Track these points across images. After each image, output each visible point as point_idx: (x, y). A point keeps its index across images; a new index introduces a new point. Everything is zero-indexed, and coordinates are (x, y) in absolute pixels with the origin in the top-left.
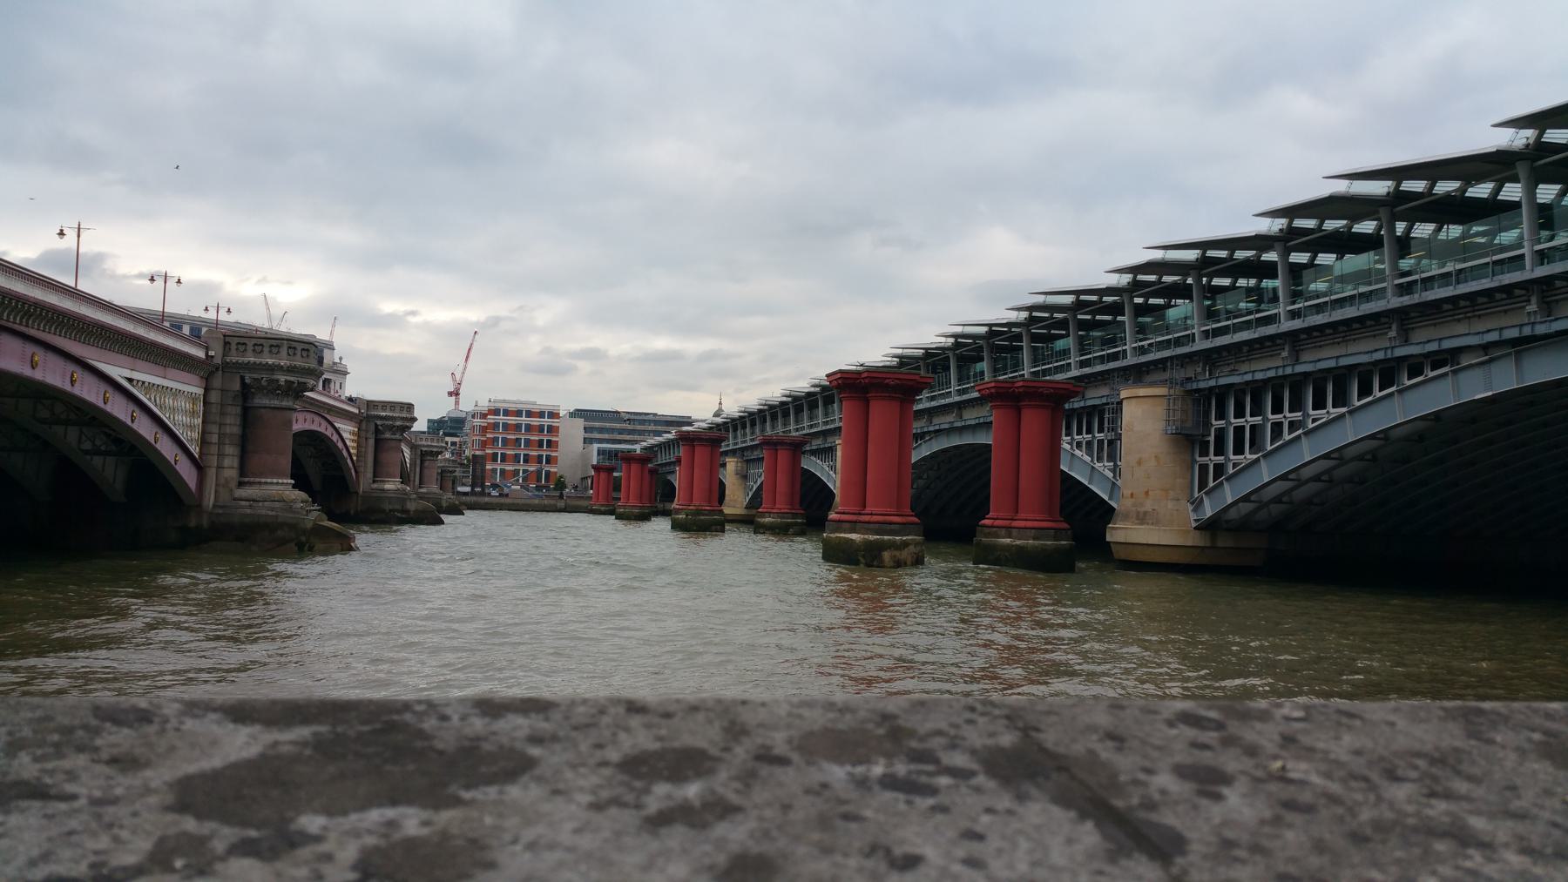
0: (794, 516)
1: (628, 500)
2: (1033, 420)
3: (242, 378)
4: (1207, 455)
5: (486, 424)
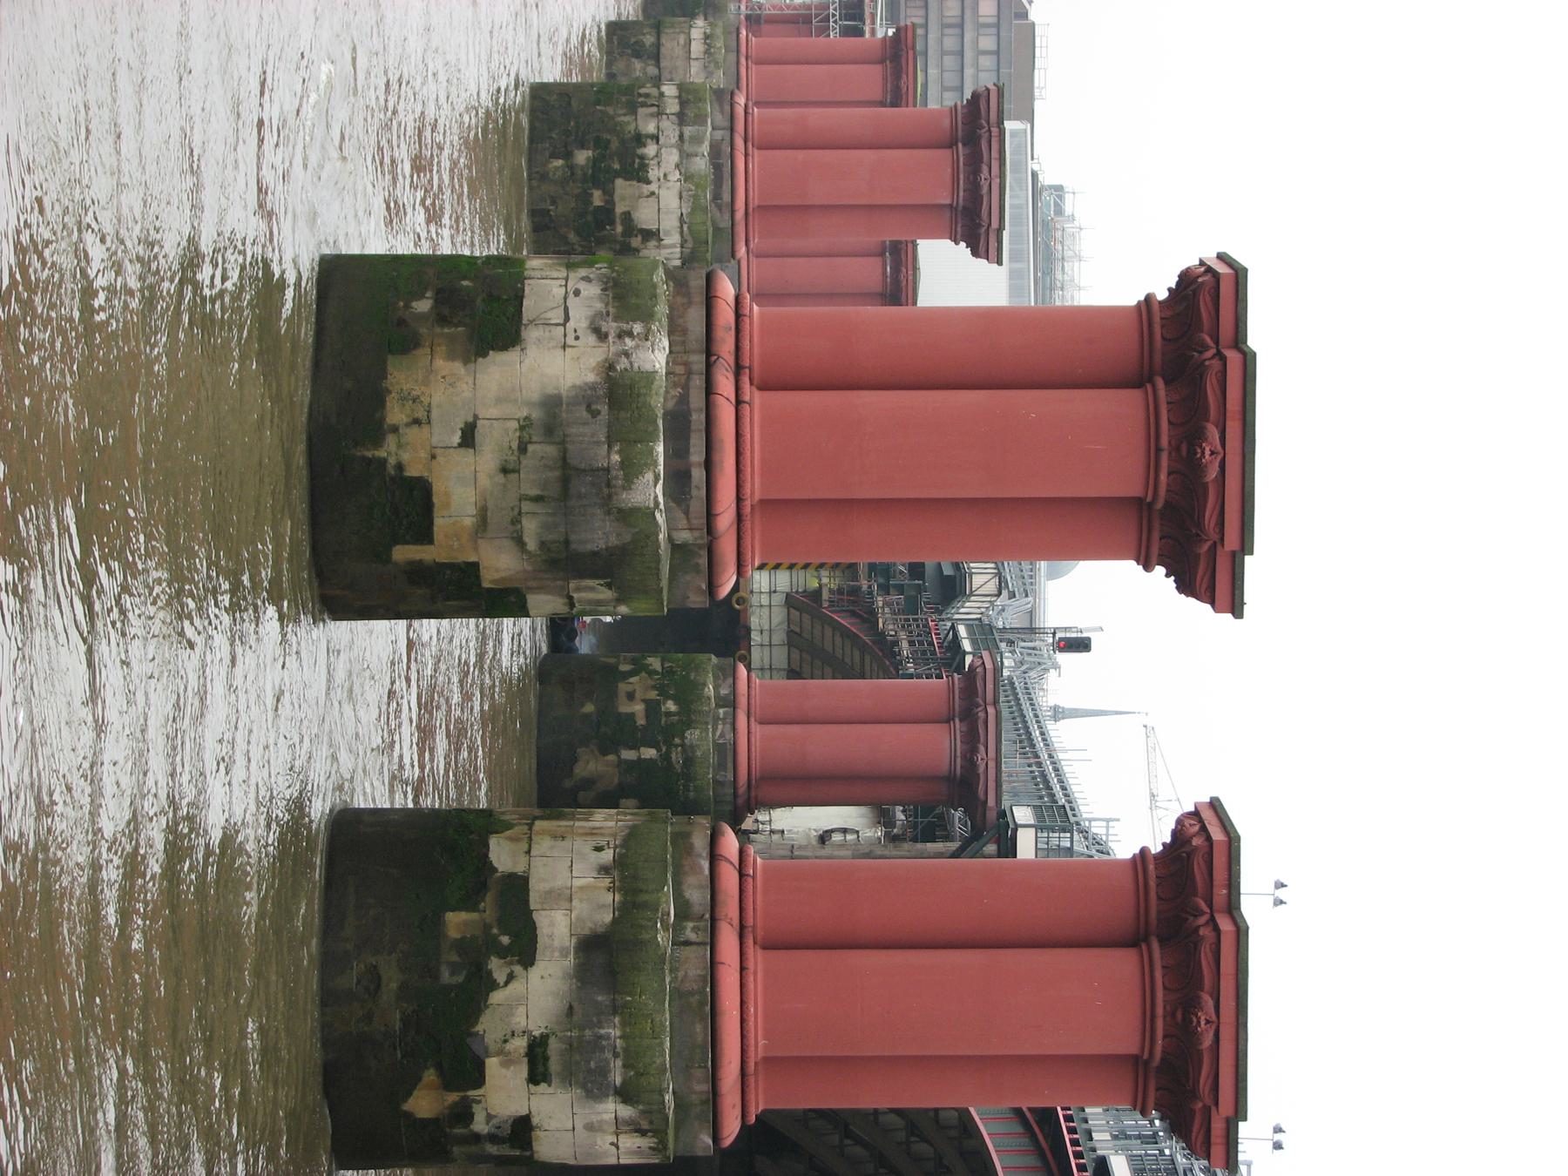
1: (759, 62)
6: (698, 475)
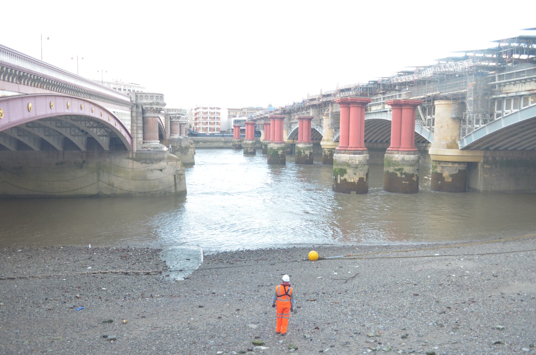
0: (310, 144)
2: (406, 113)
3: (142, 108)
4: (465, 124)
5: (196, 112)
6: (359, 152)
